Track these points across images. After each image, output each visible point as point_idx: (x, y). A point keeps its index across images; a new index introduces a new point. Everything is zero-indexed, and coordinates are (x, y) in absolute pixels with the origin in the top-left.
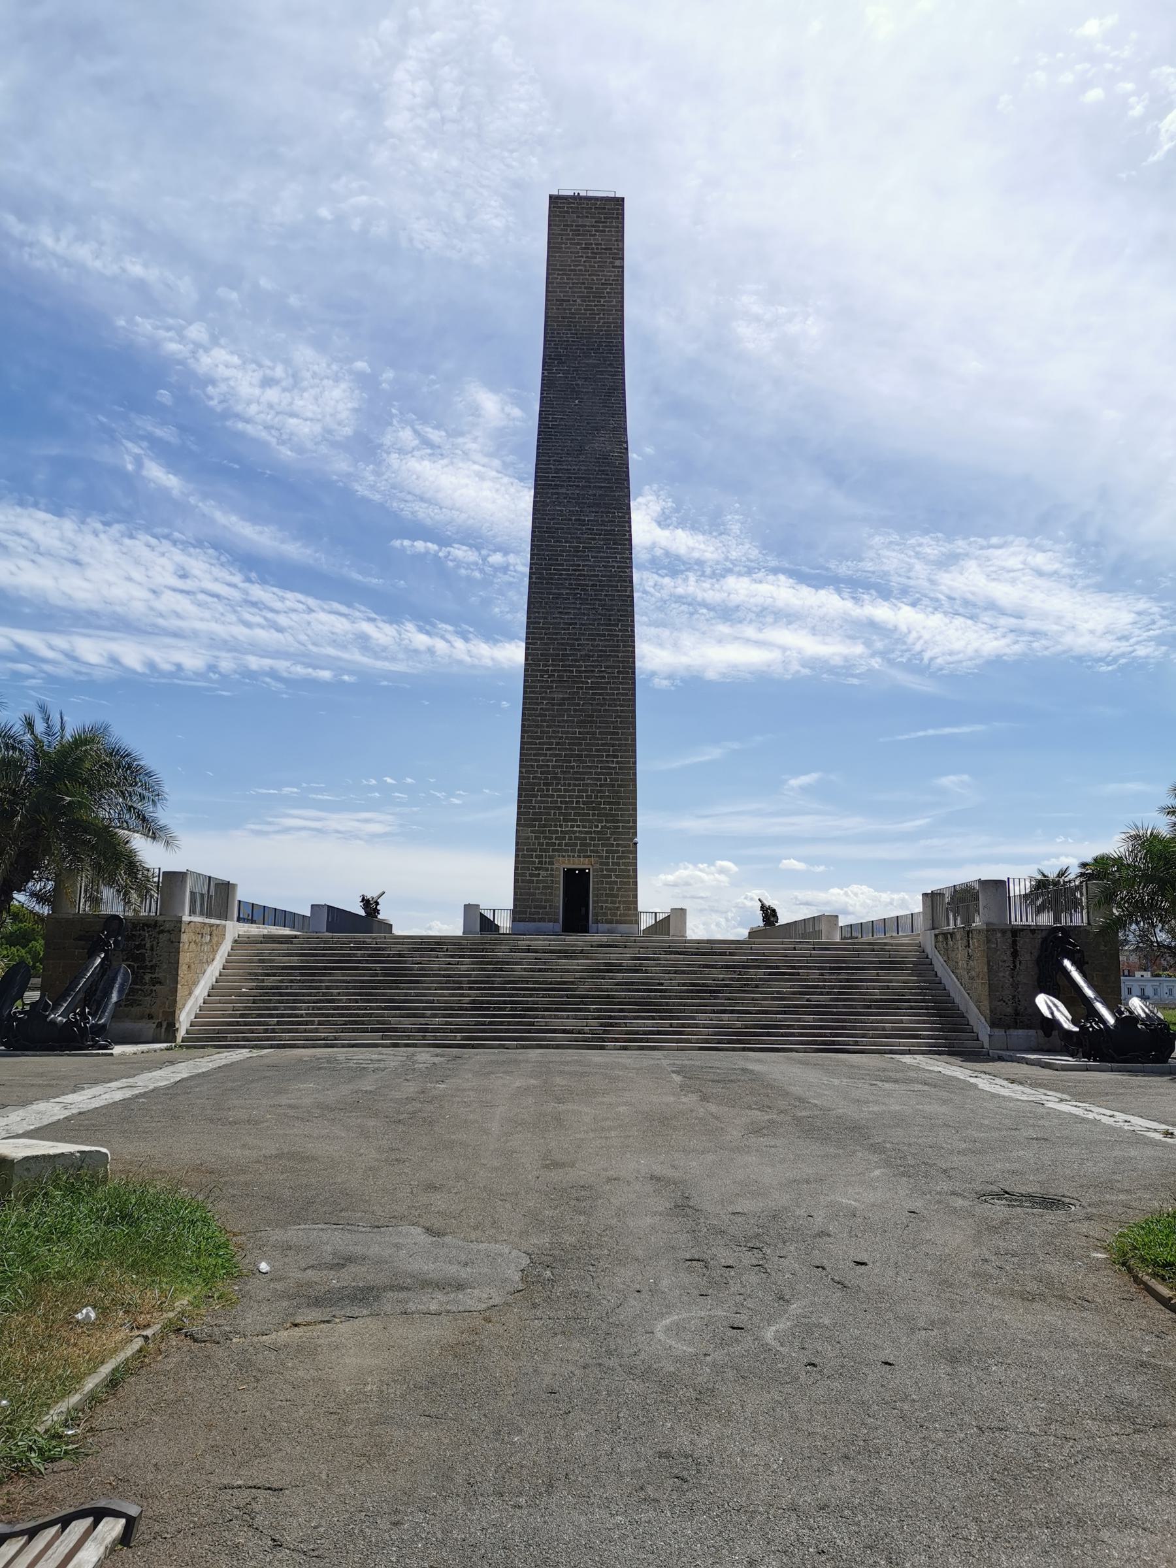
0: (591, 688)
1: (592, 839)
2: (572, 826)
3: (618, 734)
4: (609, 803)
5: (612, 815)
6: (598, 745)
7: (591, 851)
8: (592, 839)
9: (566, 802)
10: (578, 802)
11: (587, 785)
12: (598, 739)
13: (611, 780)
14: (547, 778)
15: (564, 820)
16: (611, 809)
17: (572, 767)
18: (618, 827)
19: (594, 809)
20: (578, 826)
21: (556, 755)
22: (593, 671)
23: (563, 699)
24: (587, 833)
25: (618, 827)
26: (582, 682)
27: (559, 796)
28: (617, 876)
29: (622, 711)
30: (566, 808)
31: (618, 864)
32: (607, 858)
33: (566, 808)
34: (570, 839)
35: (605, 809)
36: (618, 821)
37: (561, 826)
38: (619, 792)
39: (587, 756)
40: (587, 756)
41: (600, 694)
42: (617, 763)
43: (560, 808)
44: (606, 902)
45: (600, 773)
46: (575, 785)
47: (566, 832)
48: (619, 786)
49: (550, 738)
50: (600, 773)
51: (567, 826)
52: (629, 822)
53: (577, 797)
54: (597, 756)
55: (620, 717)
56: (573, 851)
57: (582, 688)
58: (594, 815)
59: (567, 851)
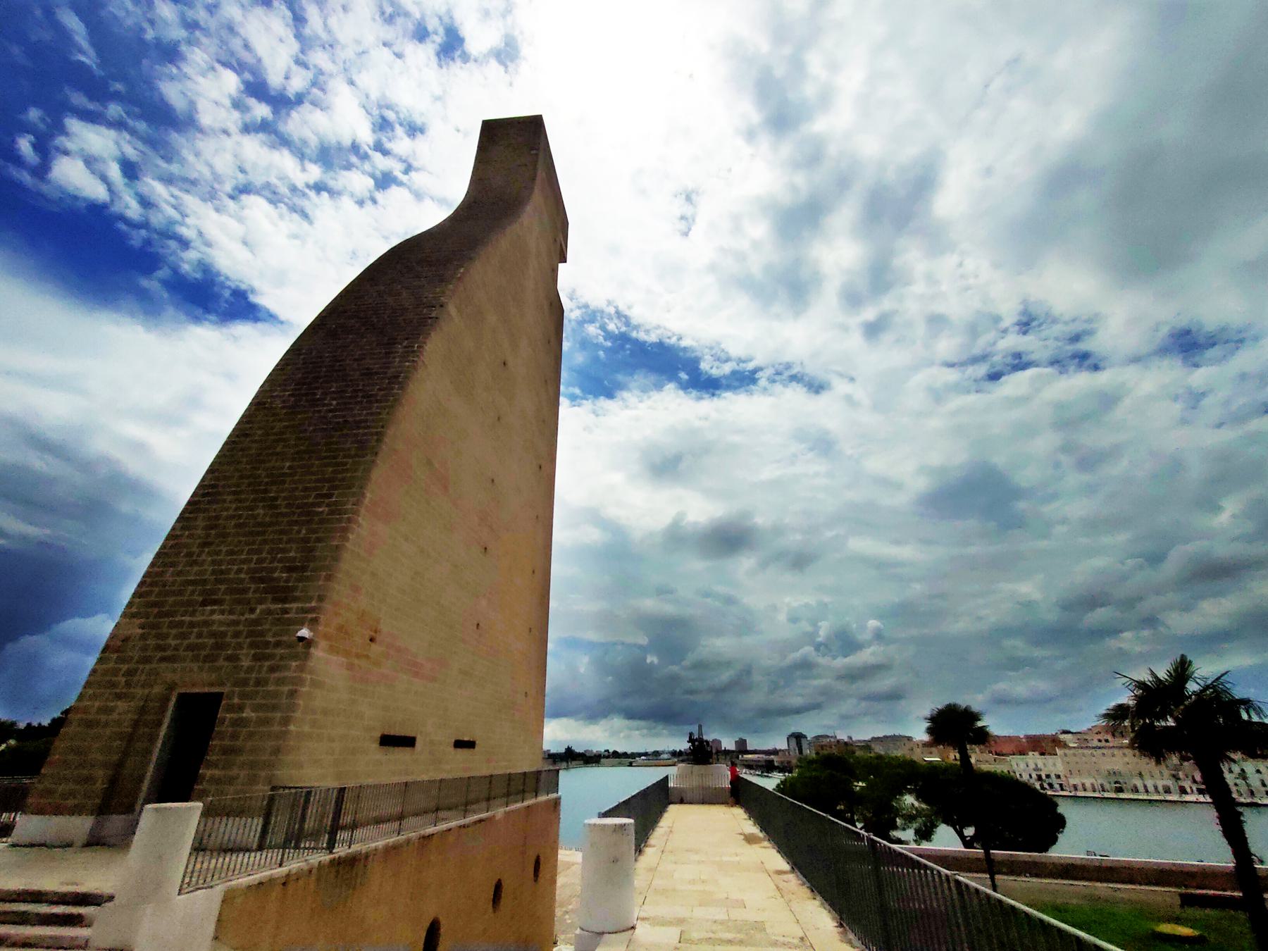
0: (330, 411)
2: (213, 612)
3: (346, 464)
7: (228, 658)
9: (222, 572)
12: (313, 474)
15: (204, 604)
17: (255, 517)
18: (286, 611)
19: (262, 580)
20: (222, 612)
28: (256, 709)
29: (365, 434)
32: (250, 670)
34: (200, 636)
36: (295, 600)
42: (328, 505)
44: (215, 765)
46: (247, 544)
47: (192, 625)
49: (241, 477)
52: (310, 599)
53: (243, 562)
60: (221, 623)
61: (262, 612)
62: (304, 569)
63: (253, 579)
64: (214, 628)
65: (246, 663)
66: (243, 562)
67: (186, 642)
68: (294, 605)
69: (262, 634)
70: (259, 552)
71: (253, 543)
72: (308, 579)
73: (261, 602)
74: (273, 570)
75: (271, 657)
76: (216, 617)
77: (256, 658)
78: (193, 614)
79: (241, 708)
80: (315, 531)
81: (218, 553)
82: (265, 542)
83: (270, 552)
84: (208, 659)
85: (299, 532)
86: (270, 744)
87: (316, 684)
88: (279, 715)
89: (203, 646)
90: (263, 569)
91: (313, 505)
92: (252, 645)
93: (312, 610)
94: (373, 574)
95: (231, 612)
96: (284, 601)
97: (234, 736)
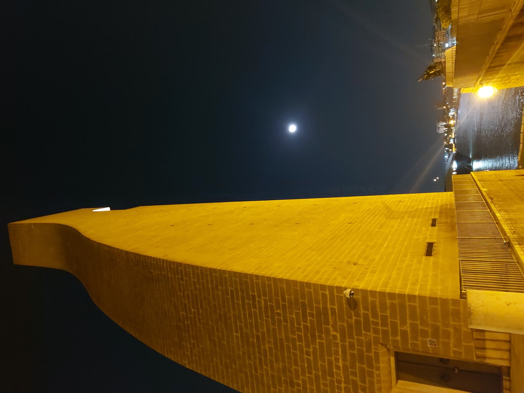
1: (352, 346)
2: (338, 368)
3: (232, 291)
4: (305, 315)
5: (319, 314)
6: (245, 315)
7: (369, 350)
8: (352, 346)
9: (309, 367)
10: (308, 353)
11: (287, 338)
13: (278, 307)
14: (285, 381)
15: (331, 375)
16: (312, 315)
19: (313, 336)
20: (337, 360)
21: (261, 363)
22: (185, 305)
23: (210, 340)
24: (344, 352)
25: (333, 310)
26: (195, 318)
27: (303, 374)
28: (404, 323)
30: (317, 370)
31: (384, 319)
32: (376, 331)
33: (317, 370)
34: (355, 374)
35: (312, 322)
36: (325, 308)
37: (339, 382)
38: (290, 301)
39: (257, 330)
40: (257, 330)
41: (201, 303)
43: (317, 377)
45: (273, 318)
46: (289, 351)
48: (284, 299)
50: (273, 318)
51: (338, 375)
52: (324, 295)
53: (302, 351)
54: (256, 317)
55: (217, 286)
56: (371, 374)
57: (199, 319)
58: (320, 337)
59: (372, 383)
60: (344, 359)
61: (335, 330)
62: (304, 305)
63: (314, 342)
64: (348, 364)
65: (372, 334)
66: (302, 351)
67: (359, 383)
68: (329, 306)
69: (350, 326)
70: (294, 340)
71: (289, 347)
72: (310, 301)
73: (328, 332)
74: (306, 327)
75: (366, 317)
76: (341, 364)
77: (367, 329)
78: (339, 382)
79: (404, 334)
80: (277, 301)
81: (297, 371)
82: (287, 338)
83: (293, 333)
84: (370, 366)
85: (279, 315)
86: (429, 307)
87: (386, 284)
88: (407, 304)
89: (362, 370)
90: (306, 336)
91: (260, 308)
92: (359, 334)
93: (332, 293)
94: (308, 266)
95: (337, 353)
96: (326, 315)
97: (424, 334)
